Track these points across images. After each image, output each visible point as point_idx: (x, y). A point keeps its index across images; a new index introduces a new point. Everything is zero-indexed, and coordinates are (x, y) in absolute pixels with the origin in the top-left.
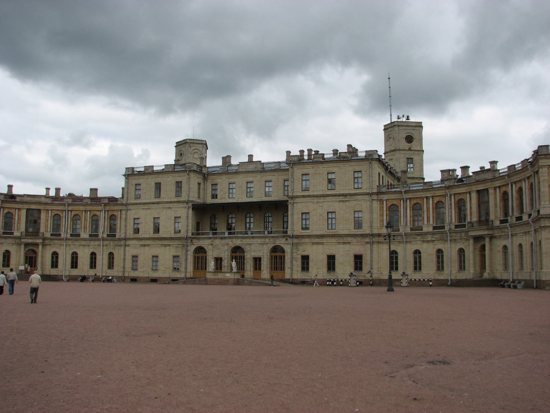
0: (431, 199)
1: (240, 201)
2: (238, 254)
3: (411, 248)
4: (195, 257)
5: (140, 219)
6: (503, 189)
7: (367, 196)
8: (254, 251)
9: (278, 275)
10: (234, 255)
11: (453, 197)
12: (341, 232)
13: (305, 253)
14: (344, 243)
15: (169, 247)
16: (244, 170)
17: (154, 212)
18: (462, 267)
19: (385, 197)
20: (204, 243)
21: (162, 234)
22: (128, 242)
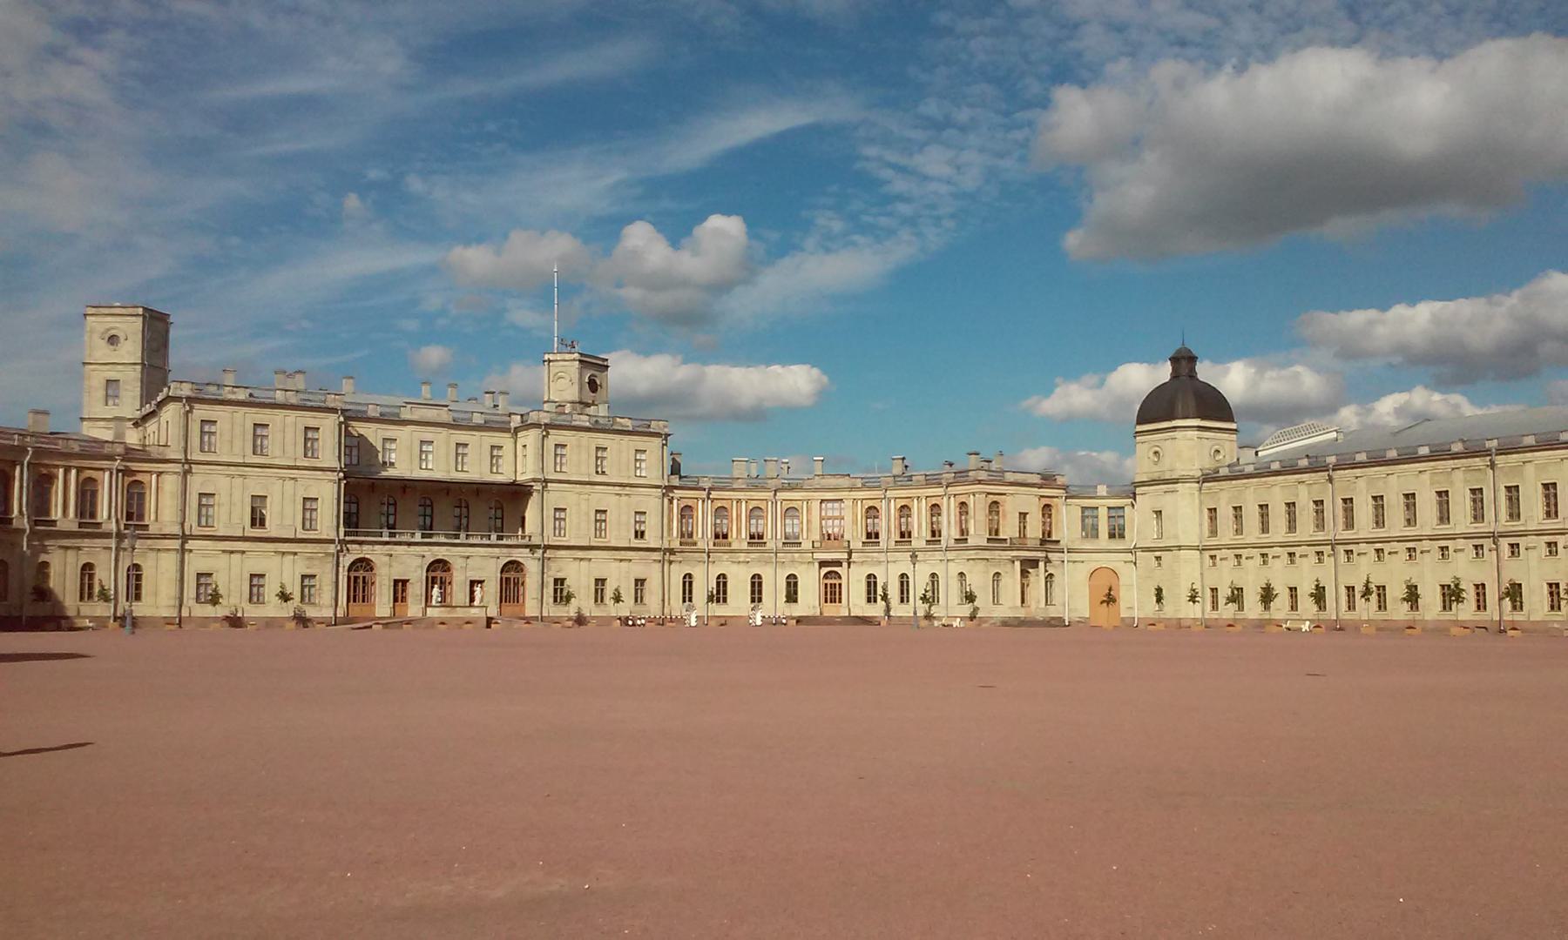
0: (744, 503)
1: (407, 474)
2: (438, 574)
3: (715, 571)
4: (349, 578)
5: (216, 496)
6: (871, 503)
7: (654, 490)
8: (473, 570)
9: (509, 608)
10: (431, 574)
11: (779, 503)
12: (613, 544)
13: (560, 575)
14: (621, 560)
15: (292, 557)
16: (415, 417)
17: (257, 483)
18: (792, 597)
19: (678, 493)
20: (375, 553)
21: (272, 529)
22: (190, 544)
